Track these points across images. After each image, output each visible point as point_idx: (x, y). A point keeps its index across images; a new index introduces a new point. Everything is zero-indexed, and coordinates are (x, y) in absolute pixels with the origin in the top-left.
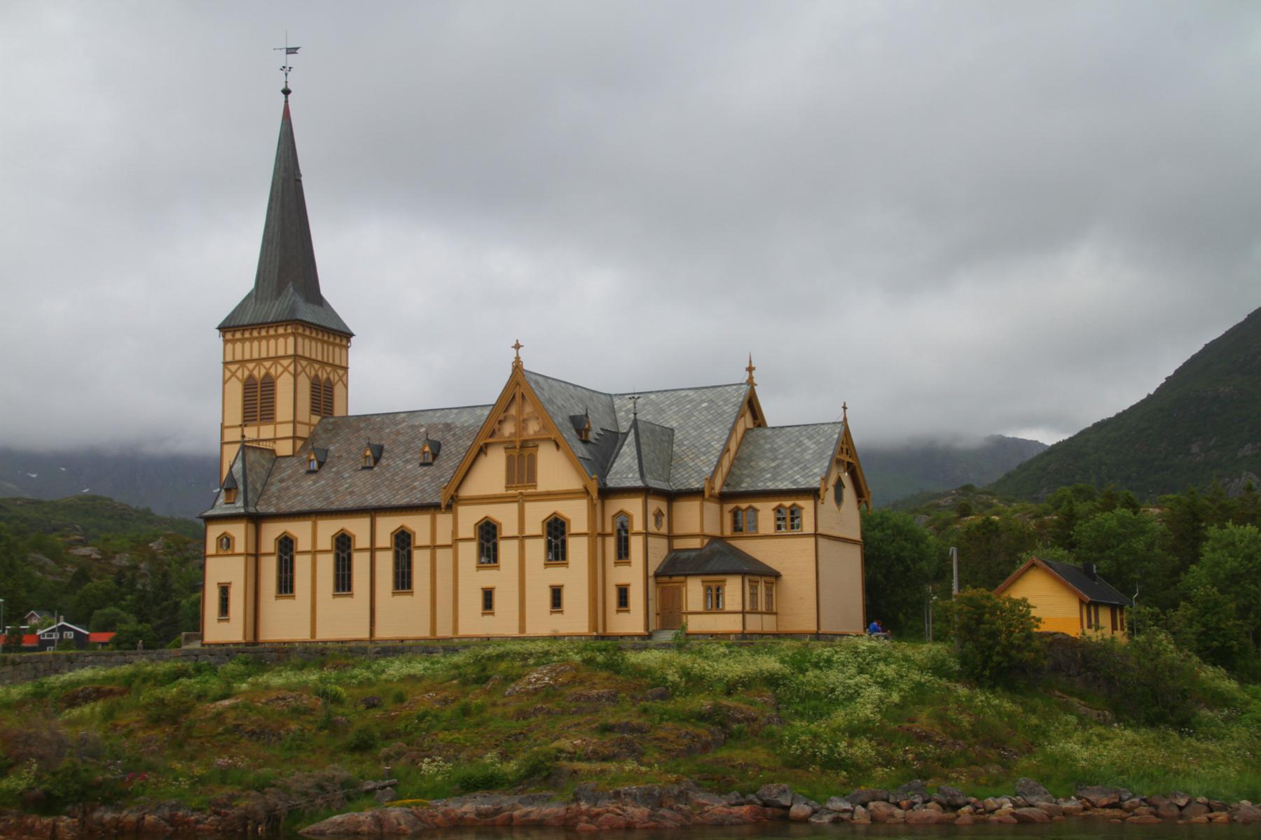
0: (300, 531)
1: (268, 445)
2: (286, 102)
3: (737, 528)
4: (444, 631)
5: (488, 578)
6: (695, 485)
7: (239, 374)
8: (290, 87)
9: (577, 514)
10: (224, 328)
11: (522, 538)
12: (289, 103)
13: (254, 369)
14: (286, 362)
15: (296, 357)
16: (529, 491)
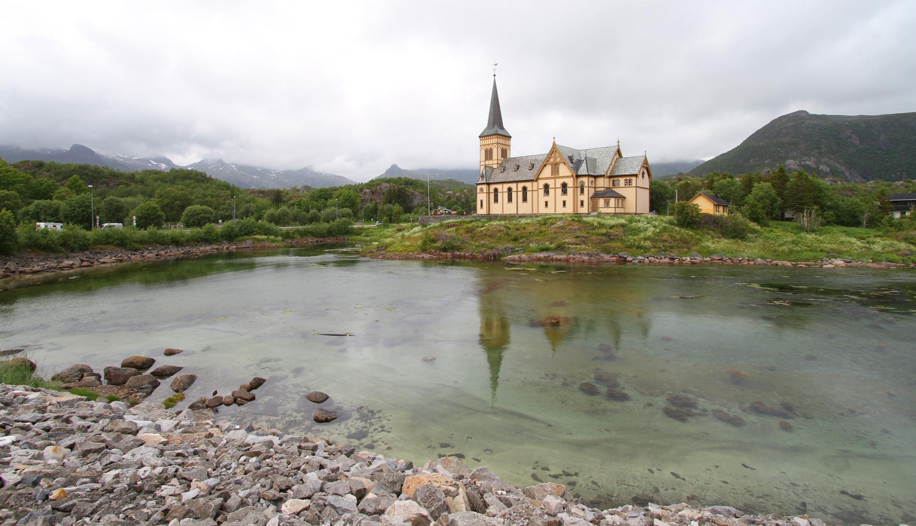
0: (499, 187)
1: (491, 166)
3: (613, 185)
4: (535, 212)
5: (546, 198)
6: (602, 174)
9: (570, 182)
10: (480, 137)
11: (555, 188)
14: (495, 145)
15: (498, 143)
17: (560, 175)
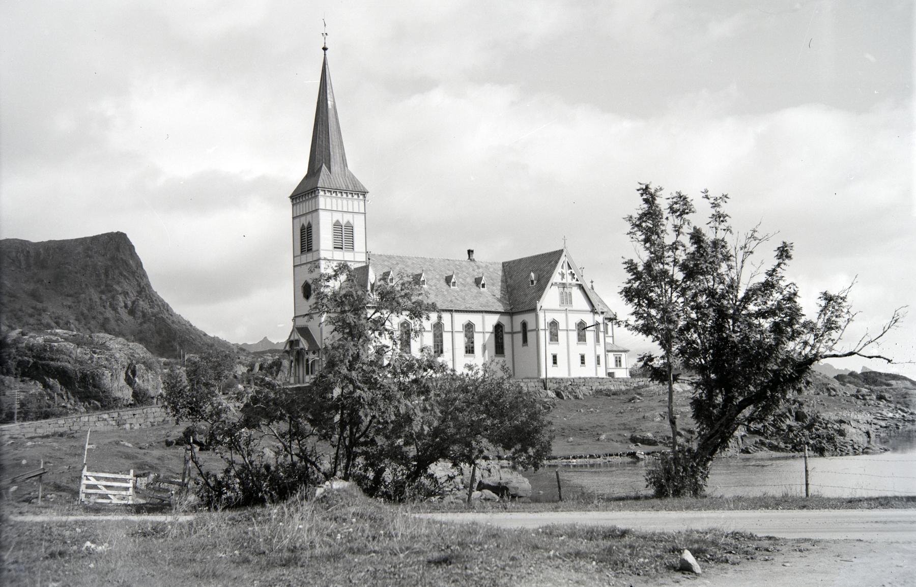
2: (325, 55)
5: (552, 349)
8: (327, 46)
12: (327, 56)
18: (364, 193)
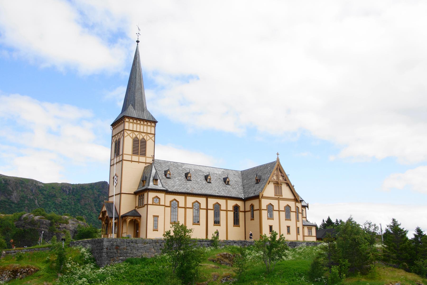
7: (131, 135)
8: (139, 40)
13: (138, 135)
14: (151, 136)
16: (280, 197)
17: (284, 197)
18: (155, 122)
